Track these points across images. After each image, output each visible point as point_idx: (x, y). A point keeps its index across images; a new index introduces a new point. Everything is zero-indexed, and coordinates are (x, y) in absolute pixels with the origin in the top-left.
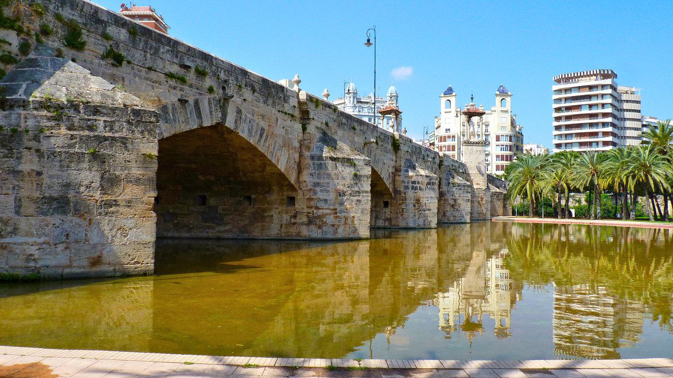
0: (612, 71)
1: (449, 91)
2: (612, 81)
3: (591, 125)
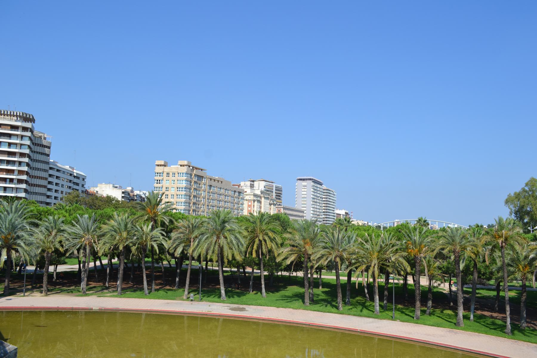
0: (33, 117)
2: (32, 125)
3: (8, 162)
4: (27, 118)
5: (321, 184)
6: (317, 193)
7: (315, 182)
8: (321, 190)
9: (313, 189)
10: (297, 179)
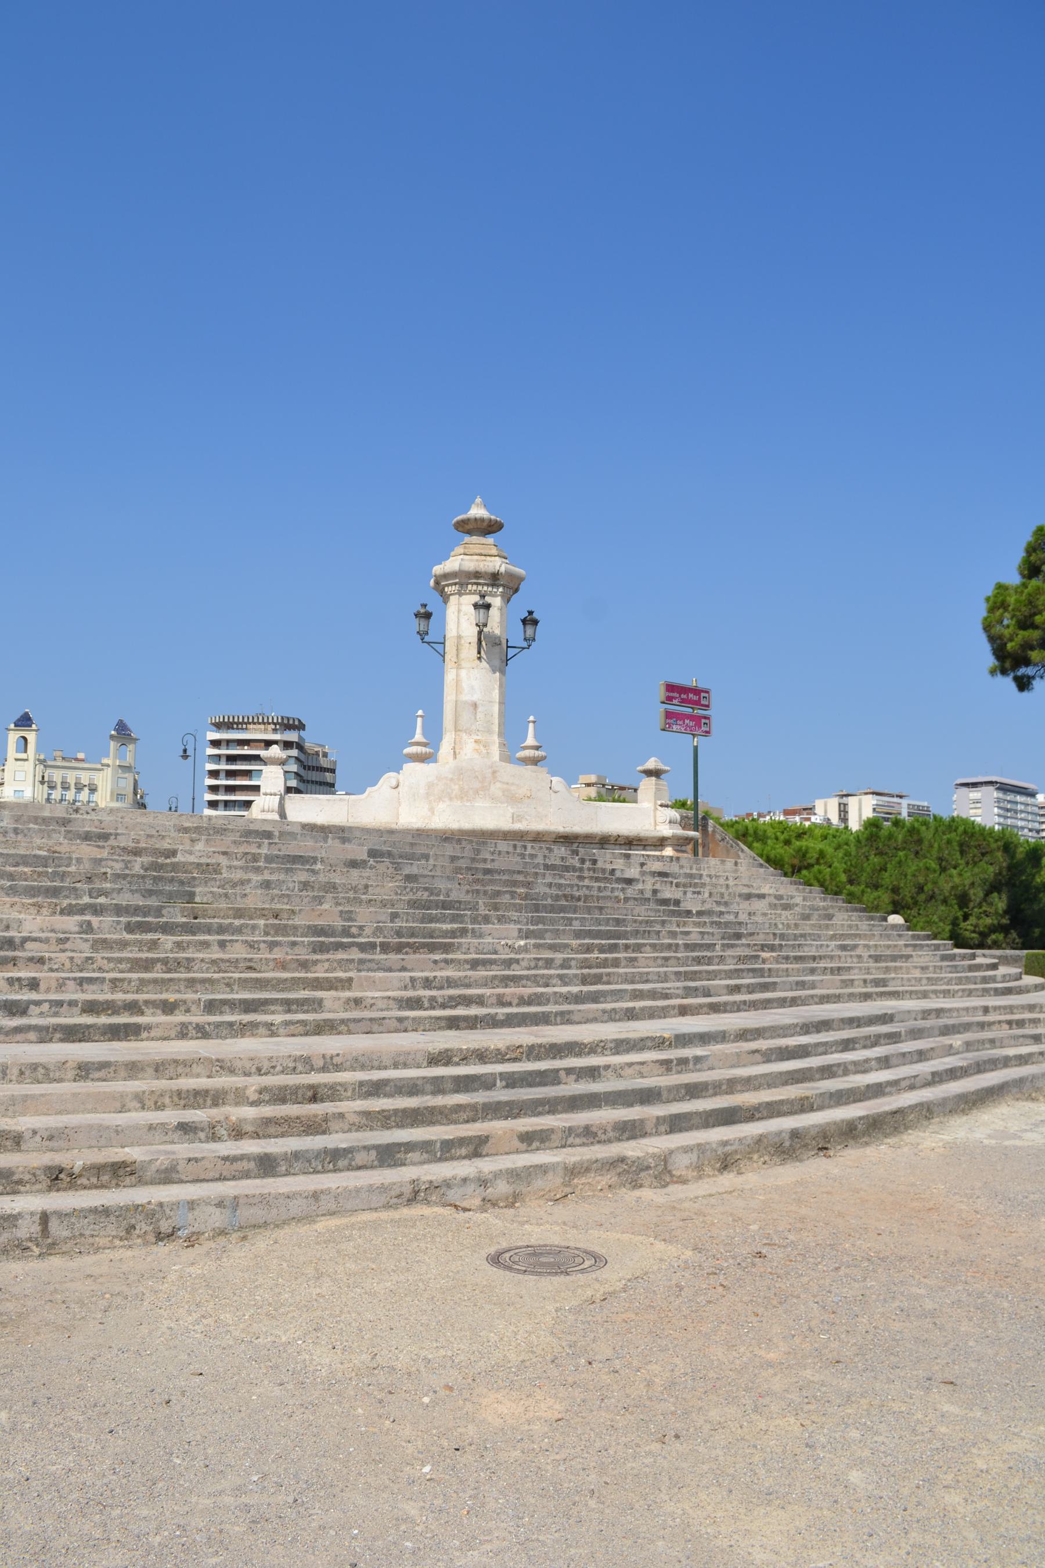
0: (299, 721)
1: (25, 721)
2: (300, 737)
4: (288, 725)
5: (1032, 795)
6: (1017, 818)
7: (1004, 788)
8: (1036, 810)
9: (999, 807)
10: (957, 785)
